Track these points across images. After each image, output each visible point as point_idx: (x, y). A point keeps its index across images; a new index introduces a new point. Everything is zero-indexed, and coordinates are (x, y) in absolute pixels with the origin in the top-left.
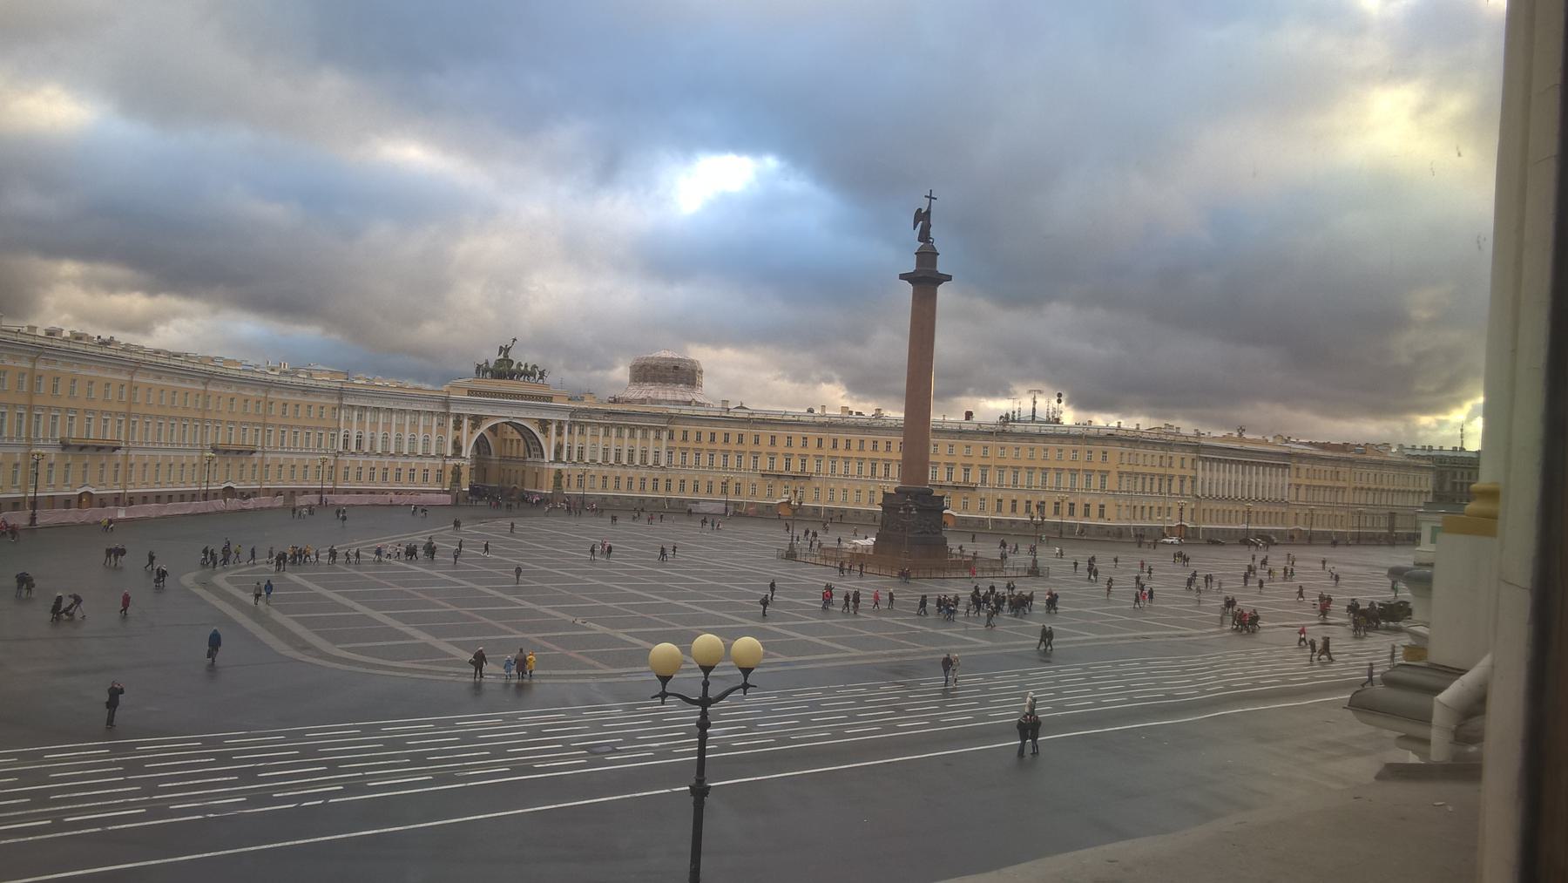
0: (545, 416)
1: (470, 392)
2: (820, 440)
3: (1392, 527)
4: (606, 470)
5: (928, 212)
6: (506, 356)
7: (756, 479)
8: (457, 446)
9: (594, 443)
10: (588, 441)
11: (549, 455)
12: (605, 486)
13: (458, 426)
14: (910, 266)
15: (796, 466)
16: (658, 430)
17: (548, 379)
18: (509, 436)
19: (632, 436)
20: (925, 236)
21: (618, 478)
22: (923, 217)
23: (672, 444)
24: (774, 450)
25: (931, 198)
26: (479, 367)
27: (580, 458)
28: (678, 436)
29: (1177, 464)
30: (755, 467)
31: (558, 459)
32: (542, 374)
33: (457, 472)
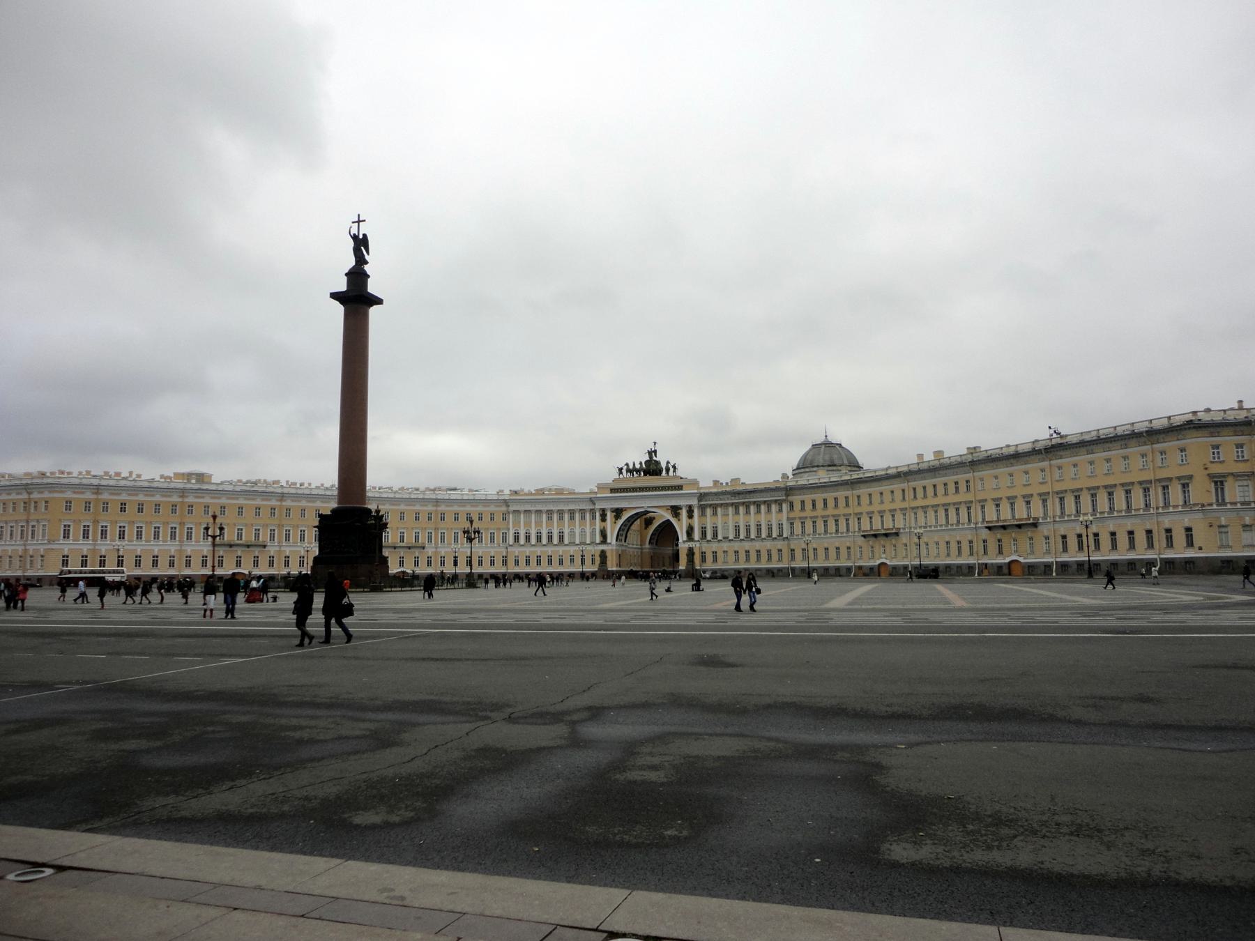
1: (613, 490)
4: (736, 546)
9: (725, 521)
10: (719, 521)
11: (682, 536)
12: (737, 560)
13: (603, 519)
15: (889, 524)
16: (779, 503)
17: (679, 473)
21: (747, 552)
23: (792, 515)
27: (715, 535)
28: (797, 506)
32: (674, 467)
33: (603, 555)
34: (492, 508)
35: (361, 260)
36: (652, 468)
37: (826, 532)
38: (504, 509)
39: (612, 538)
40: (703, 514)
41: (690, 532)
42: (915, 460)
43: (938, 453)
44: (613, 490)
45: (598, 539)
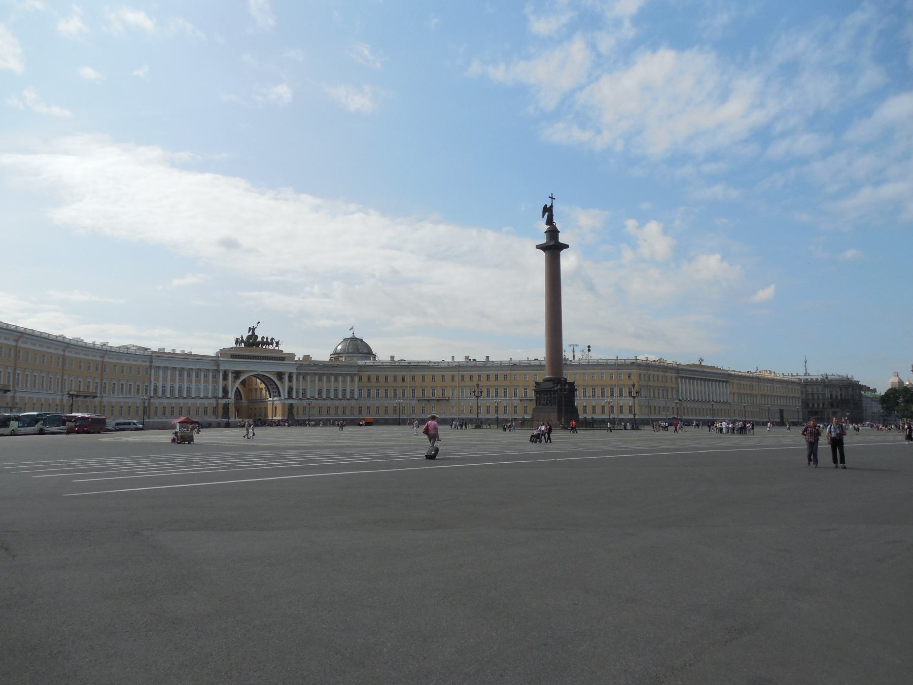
0: (280, 370)
1: (233, 356)
2: (453, 377)
3: (782, 417)
4: (321, 403)
5: (552, 206)
6: (253, 333)
7: (414, 403)
8: (225, 391)
9: (312, 387)
13: (225, 377)
14: (543, 240)
15: (438, 393)
18: (254, 387)
19: (336, 380)
20: (550, 221)
22: (548, 211)
24: (424, 384)
25: (552, 198)
26: (237, 339)
29: (669, 380)
30: (413, 396)
31: (290, 396)
32: (277, 343)
34: (139, 363)
35: (550, 221)
36: (252, 341)
37: (369, 396)
38: (148, 364)
39: (231, 395)
40: (297, 380)
41: (290, 390)
42: (450, 360)
43: (467, 357)
44: (233, 356)
45: (221, 395)
